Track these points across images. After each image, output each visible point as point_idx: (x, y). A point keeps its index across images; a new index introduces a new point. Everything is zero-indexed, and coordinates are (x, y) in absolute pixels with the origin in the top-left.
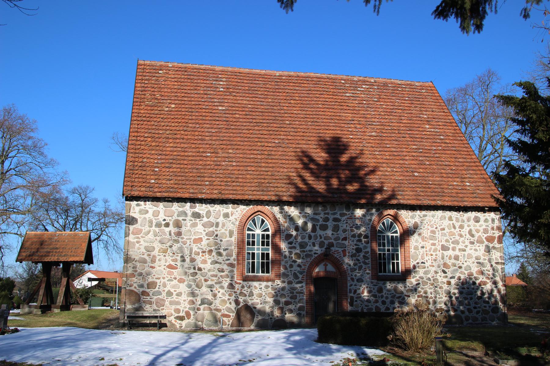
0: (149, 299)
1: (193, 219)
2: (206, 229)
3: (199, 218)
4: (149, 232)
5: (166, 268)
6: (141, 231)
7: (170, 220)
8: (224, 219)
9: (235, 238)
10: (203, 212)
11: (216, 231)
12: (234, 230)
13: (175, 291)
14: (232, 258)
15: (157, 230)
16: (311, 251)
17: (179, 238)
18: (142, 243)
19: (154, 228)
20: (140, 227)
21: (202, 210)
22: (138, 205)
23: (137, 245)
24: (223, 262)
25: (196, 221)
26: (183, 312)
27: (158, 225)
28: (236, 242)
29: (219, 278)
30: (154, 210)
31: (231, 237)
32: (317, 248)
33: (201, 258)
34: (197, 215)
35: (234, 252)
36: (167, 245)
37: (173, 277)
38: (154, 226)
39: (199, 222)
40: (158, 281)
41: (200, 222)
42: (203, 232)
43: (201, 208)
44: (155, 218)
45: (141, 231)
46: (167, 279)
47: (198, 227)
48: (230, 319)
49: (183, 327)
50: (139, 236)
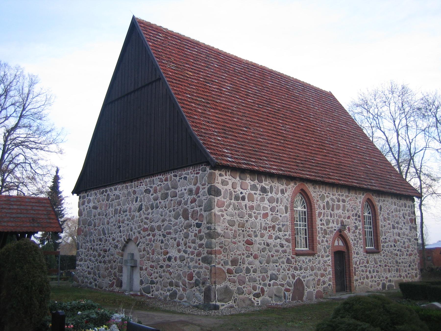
0: (232, 277)
1: (261, 193)
2: (270, 204)
3: (266, 193)
4: (230, 204)
5: (245, 244)
6: (224, 203)
7: (245, 193)
8: (281, 195)
9: (289, 214)
10: (268, 187)
11: (277, 206)
12: (288, 206)
13: (252, 267)
14: (287, 233)
15: (236, 202)
16: (332, 227)
17: (252, 212)
18: (225, 216)
19: (233, 201)
20: (223, 199)
21: (267, 185)
22: (221, 175)
23: (222, 218)
24: (282, 238)
25: (264, 196)
26: (259, 289)
27: (237, 198)
28: (290, 218)
29: (281, 253)
30: (233, 181)
31: (286, 213)
32: (335, 224)
33: (268, 233)
34: (264, 190)
35: (289, 227)
36: (244, 220)
37: (250, 252)
38: (233, 199)
39: (266, 197)
40: (239, 257)
41: (267, 197)
42: (268, 207)
43: (266, 183)
44: (172, 206)
45: (224, 203)
46: (246, 255)
47: (265, 202)
48: (290, 293)
49: (259, 304)
50: (223, 208)
